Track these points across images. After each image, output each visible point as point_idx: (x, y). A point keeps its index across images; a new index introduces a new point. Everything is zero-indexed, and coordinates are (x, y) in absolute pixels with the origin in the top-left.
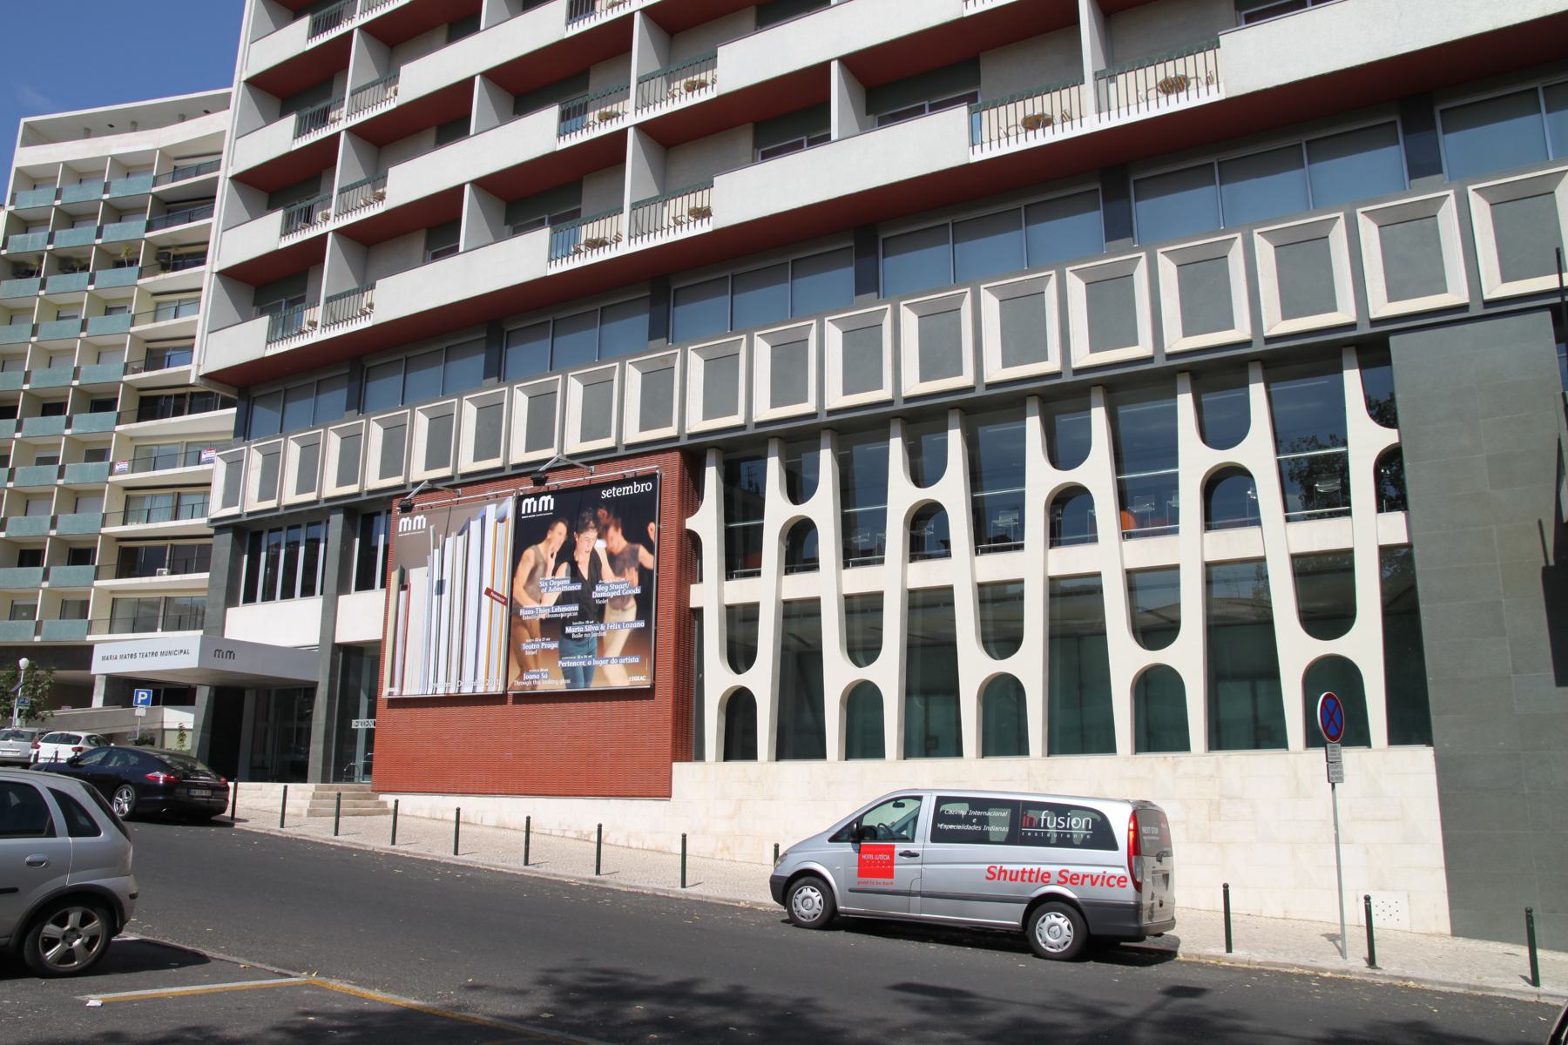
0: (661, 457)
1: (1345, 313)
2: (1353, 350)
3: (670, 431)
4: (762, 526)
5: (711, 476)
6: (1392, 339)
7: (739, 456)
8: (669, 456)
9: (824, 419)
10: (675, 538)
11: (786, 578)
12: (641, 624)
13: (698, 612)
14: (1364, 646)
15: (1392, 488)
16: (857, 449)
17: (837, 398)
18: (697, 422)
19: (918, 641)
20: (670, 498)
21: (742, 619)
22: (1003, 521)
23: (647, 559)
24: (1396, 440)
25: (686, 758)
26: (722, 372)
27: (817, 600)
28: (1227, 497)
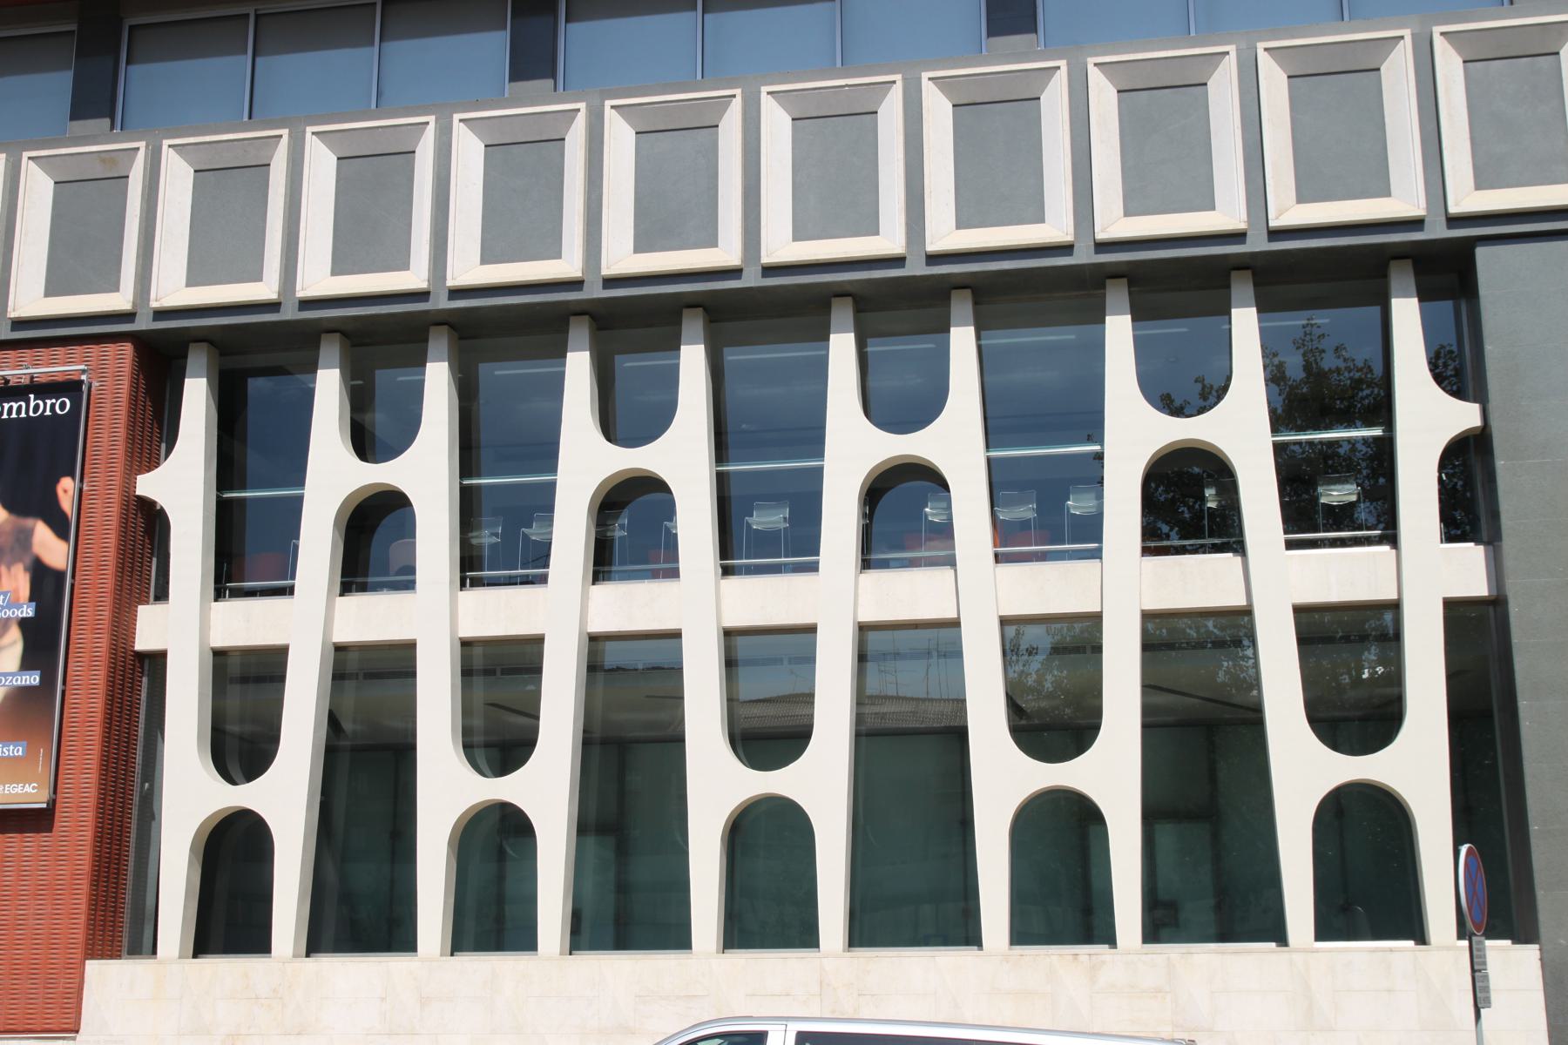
0: (94, 350)
1: (1405, 199)
2: (1408, 265)
3: (119, 301)
4: (298, 501)
5: (196, 397)
6: (1482, 253)
7: (255, 362)
8: (111, 349)
9: (442, 303)
10: (115, 510)
11: (340, 600)
12: (33, 679)
13: (156, 661)
14: (1417, 765)
15: (1467, 506)
16: (484, 368)
17: (468, 267)
18: (174, 288)
19: (597, 735)
20: (108, 428)
21: (246, 680)
22: (1077, 505)
23: (51, 548)
24: (1476, 421)
25: (110, 951)
26: (230, 194)
27: (409, 647)
28: (1189, 503)
